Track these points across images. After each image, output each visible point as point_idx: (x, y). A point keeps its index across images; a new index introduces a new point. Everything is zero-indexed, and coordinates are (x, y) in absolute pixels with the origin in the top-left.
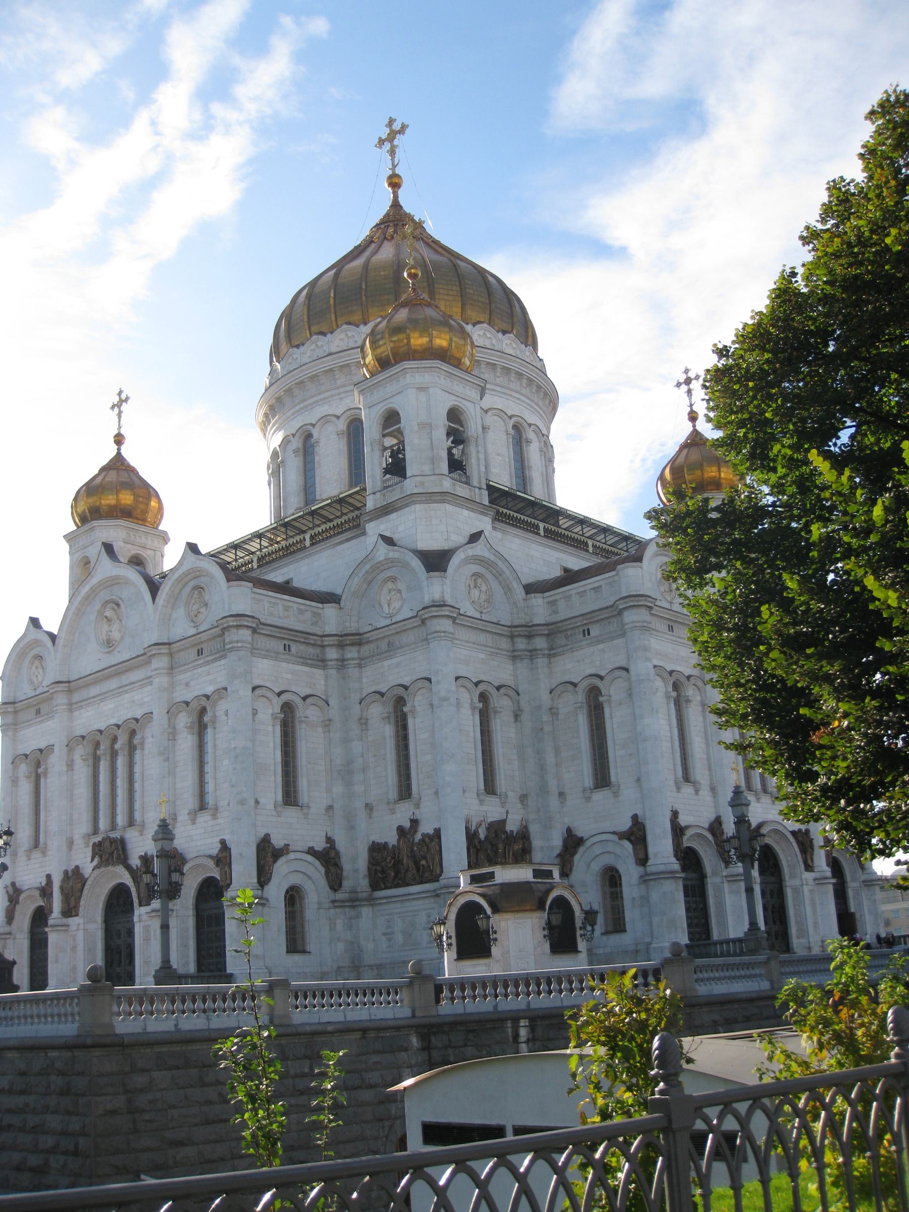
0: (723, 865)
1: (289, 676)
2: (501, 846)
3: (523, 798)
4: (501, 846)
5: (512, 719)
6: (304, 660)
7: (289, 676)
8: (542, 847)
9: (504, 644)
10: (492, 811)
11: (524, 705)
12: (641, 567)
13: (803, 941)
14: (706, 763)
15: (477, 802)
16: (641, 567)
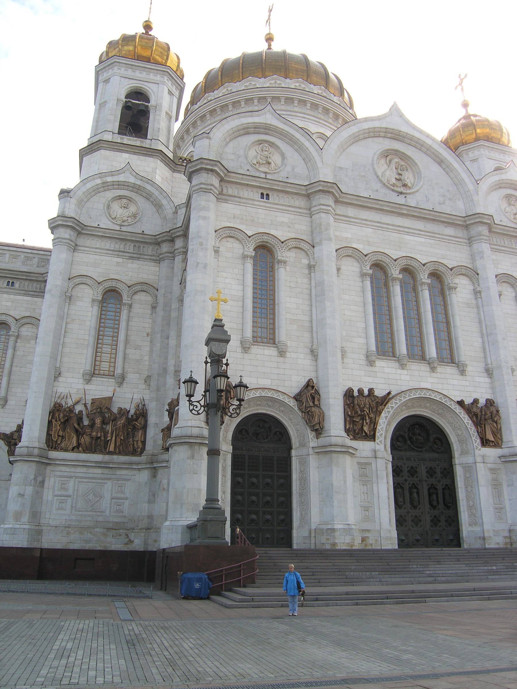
0: (311, 435)
1: (9, 304)
2: (98, 421)
3: (147, 380)
4: (98, 421)
5: (149, 312)
6: (26, 293)
7: (9, 304)
8: (156, 424)
9: (149, 250)
10: (101, 389)
11: (161, 300)
12: (210, 138)
13: (477, 529)
14: (307, 324)
15: (81, 381)
16: (210, 138)
